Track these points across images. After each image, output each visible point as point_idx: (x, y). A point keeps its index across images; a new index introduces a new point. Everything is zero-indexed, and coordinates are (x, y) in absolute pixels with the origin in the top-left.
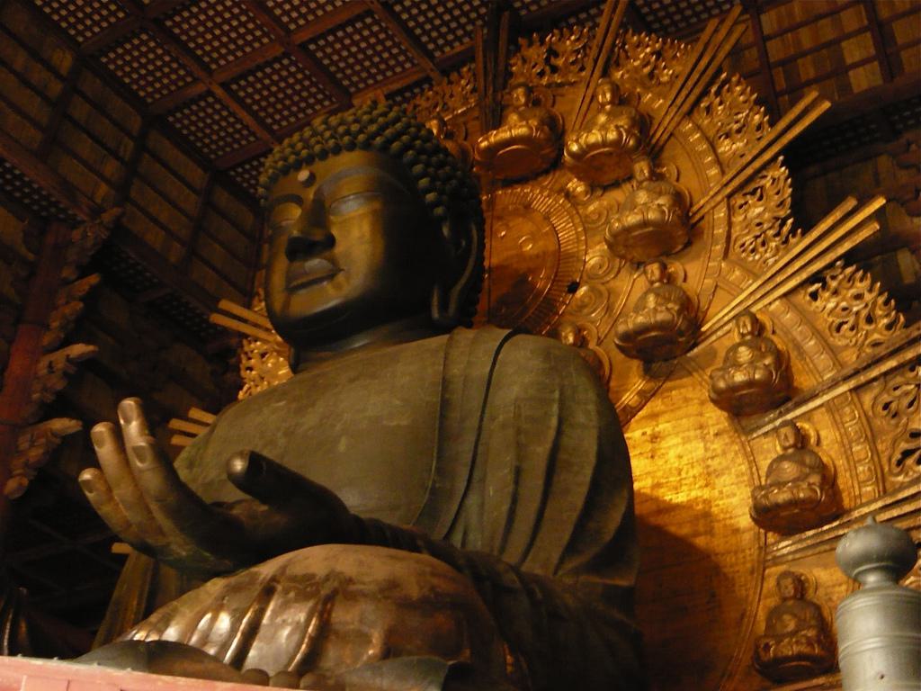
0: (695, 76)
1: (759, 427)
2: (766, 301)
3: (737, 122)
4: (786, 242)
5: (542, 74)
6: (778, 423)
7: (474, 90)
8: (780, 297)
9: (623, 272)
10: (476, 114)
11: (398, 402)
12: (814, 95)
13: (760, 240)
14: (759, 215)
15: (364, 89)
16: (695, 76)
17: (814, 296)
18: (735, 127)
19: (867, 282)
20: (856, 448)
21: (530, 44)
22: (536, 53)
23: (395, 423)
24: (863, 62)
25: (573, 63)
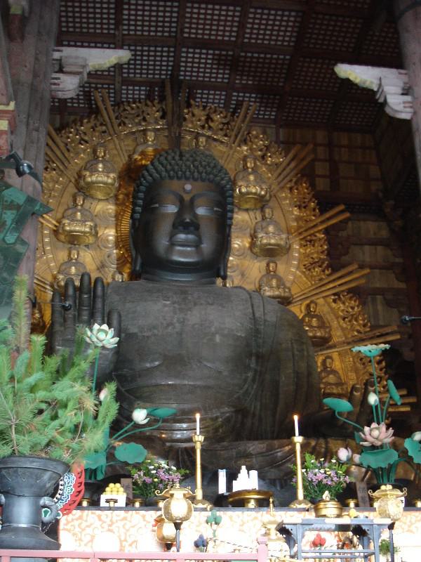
2: (318, 297)
4: (324, 271)
5: (203, 127)
6: (320, 353)
7: (163, 117)
8: (324, 297)
9: (248, 257)
10: (166, 134)
11: (239, 324)
12: (342, 207)
14: (312, 253)
17: (335, 301)
18: (303, 205)
19: (357, 303)
20: (350, 374)
23: (239, 334)
24: (323, 176)
25: (221, 130)
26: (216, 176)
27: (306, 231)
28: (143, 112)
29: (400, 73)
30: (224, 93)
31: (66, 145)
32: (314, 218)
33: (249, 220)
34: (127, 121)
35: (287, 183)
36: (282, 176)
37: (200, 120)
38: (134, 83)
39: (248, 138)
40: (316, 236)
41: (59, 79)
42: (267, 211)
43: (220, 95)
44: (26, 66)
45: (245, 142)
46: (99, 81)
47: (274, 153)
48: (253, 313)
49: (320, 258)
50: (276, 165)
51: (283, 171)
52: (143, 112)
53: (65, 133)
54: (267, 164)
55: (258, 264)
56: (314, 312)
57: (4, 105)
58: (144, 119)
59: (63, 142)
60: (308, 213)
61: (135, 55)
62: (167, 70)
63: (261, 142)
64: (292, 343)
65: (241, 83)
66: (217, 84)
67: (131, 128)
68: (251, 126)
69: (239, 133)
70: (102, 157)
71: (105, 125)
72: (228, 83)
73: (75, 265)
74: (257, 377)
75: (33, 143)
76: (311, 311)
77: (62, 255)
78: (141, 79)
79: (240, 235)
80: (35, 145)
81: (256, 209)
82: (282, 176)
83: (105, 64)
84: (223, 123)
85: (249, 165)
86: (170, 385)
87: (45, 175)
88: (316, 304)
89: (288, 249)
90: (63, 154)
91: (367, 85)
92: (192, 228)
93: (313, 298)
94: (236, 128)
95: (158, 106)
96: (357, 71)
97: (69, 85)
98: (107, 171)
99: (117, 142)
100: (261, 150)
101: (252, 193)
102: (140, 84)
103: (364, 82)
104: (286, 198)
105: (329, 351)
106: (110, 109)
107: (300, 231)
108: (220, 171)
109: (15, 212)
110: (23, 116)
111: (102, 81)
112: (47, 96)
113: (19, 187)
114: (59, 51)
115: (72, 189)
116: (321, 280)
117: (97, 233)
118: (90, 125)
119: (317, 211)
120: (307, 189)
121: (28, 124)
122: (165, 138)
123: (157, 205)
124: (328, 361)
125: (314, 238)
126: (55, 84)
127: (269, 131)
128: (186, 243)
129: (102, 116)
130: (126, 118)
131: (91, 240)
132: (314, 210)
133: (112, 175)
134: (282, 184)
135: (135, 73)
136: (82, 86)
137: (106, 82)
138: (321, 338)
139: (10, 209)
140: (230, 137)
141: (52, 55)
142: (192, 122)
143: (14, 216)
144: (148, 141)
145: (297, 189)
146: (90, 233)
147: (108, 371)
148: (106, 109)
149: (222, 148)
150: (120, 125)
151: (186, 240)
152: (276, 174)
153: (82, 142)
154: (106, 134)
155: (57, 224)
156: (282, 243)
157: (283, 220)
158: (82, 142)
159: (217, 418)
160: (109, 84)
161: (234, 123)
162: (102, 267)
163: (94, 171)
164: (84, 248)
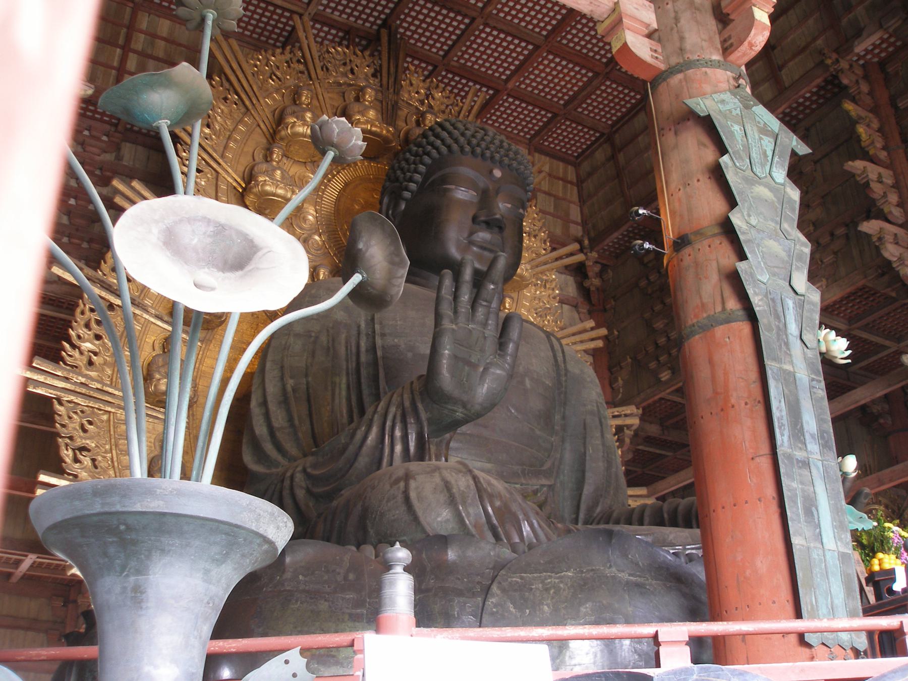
7: (374, 76)
28: (350, 61)
37: (417, 93)
64: (598, 406)
65: (457, 61)
87: (222, 107)
92: (496, 229)
95: (369, 60)
118: (283, 58)
123: (453, 187)
128: (489, 246)
129: (301, 49)
130: (330, 62)
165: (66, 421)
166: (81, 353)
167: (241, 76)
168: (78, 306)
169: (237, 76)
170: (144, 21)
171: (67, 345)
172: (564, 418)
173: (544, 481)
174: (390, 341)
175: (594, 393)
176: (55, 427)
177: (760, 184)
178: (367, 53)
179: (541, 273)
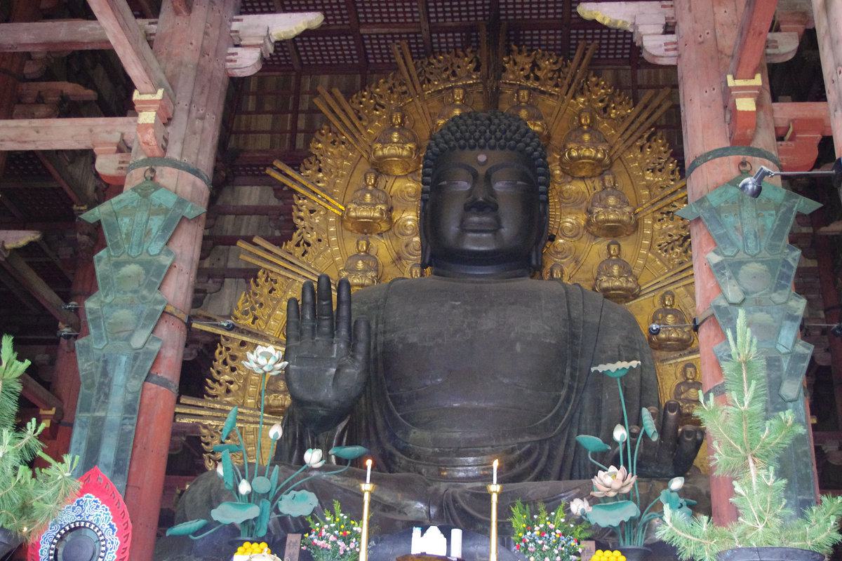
0: (637, 124)
1: (667, 360)
2: (675, 286)
3: (659, 164)
5: (527, 78)
6: (679, 360)
7: (477, 69)
11: (546, 327)
13: (671, 246)
14: (670, 229)
15: (371, 23)
16: (637, 124)
18: (658, 167)
21: (520, 52)
22: (524, 60)
23: (548, 341)
25: (551, 79)
26: (519, 141)
27: (662, 199)
29: (664, 6)
30: (558, 32)
31: (359, 111)
32: (672, 183)
33: (586, 191)
34: (431, 77)
35: (637, 141)
36: (629, 132)
38: (447, 30)
39: (586, 86)
40: (675, 206)
41: (236, 54)
42: (607, 177)
43: (555, 34)
44: (191, 44)
45: (581, 92)
46: (402, 31)
47: (621, 103)
48: (569, 311)
49: (682, 236)
50: (622, 117)
51: (630, 125)
52: (452, 64)
53: (356, 98)
54: (610, 118)
55: (598, 246)
56: (671, 306)
57: (151, 93)
58: (454, 74)
59: (353, 109)
60: (665, 177)
61: (326, 15)
62: (484, 10)
63: (603, 91)
66: (548, 21)
67: (437, 85)
68: (589, 73)
69: (573, 81)
70: (400, 124)
71: (404, 84)
72: (562, 19)
73: (362, 259)
74: (573, 396)
75: (195, 134)
76: (666, 305)
77: (351, 247)
78: (453, 24)
79: (573, 210)
80: (198, 136)
81: (595, 177)
82: (629, 132)
83: (292, 31)
84: (552, 71)
85: (583, 121)
86: (454, 408)
87: (331, 150)
88: (673, 297)
89: (636, 226)
90: (352, 122)
91: (619, 25)
93: (671, 288)
94: (569, 75)
95: (472, 55)
96: (606, 9)
97: (246, 61)
98: (402, 143)
99: (419, 104)
100: (602, 101)
101: (584, 157)
102: (453, 30)
103: (616, 22)
104: (635, 160)
105: (691, 357)
106: (411, 64)
107: (653, 201)
108: (523, 136)
109: (162, 217)
110: (184, 104)
111: (406, 30)
112: (220, 75)
113: (172, 187)
114: (238, 20)
115: (364, 166)
116: (681, 263)
117: (390, 220)
118: (387, 86)
119: (677, 173)
120: (664, 146)
121: (189, 111)
122: (479, 95)
124: (690, 370)
125: (673, 209)
126: (231, 61)
127: (622, 73)
130: (431, 73)
131: (384, 226)
132: (673, 172)
133: (408, 146)
134: (629, 143)
135: (445, 17)
136: (263, 59)
137: (412, 30)
138: (678, 340)
139: (157, 215)
140: (561, 87)
141: (230, 26)
142: (513, 72)
143: (160, 222)
144: (455, 101)
145: (650, 147)
146: (381, 219)
147: (353, 394)
148: (405, 62)
149: (551, 102)
150: (422, 84)
151: (480, 224)
152: (622, 129)
153: (378, 107)
154: (406, 95)
155: (343, 208)
156: (625, 218)
157: (631, 187)
158: (378, 107)
159: (513, 450)
160: (415, 34)
161: (566, 70)
162: (398, 259)
163: (386, 141)
164: (377, 237)
165: (209, 439)
166: (221, 385)
167: (342, 116)
168: (216, 348)
169: (340, 120)
170: (307, 83)
171: (209, 381)
172: (574, 369)
173: (527, 438)
174: (389, 336)
175: (617, 338)
176: (202, 447)
177: (129, 263)
178: (469, 50)
179: (667, 205)
